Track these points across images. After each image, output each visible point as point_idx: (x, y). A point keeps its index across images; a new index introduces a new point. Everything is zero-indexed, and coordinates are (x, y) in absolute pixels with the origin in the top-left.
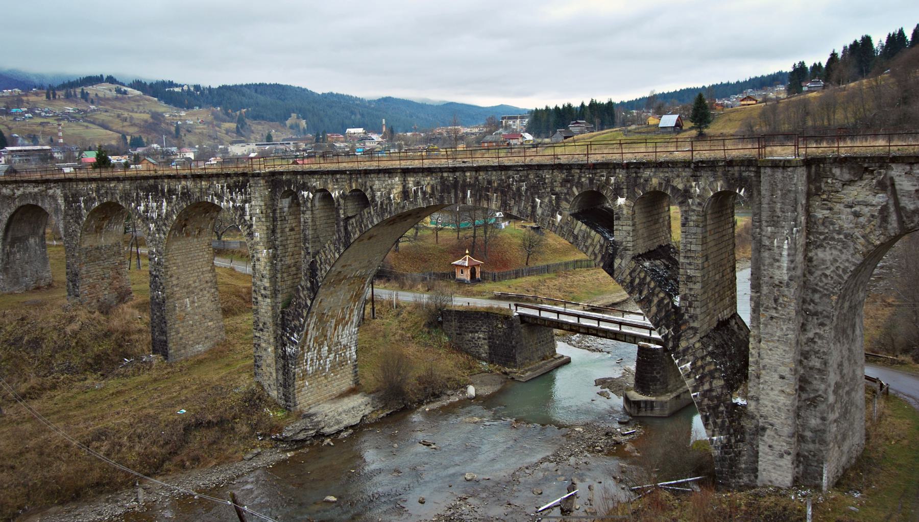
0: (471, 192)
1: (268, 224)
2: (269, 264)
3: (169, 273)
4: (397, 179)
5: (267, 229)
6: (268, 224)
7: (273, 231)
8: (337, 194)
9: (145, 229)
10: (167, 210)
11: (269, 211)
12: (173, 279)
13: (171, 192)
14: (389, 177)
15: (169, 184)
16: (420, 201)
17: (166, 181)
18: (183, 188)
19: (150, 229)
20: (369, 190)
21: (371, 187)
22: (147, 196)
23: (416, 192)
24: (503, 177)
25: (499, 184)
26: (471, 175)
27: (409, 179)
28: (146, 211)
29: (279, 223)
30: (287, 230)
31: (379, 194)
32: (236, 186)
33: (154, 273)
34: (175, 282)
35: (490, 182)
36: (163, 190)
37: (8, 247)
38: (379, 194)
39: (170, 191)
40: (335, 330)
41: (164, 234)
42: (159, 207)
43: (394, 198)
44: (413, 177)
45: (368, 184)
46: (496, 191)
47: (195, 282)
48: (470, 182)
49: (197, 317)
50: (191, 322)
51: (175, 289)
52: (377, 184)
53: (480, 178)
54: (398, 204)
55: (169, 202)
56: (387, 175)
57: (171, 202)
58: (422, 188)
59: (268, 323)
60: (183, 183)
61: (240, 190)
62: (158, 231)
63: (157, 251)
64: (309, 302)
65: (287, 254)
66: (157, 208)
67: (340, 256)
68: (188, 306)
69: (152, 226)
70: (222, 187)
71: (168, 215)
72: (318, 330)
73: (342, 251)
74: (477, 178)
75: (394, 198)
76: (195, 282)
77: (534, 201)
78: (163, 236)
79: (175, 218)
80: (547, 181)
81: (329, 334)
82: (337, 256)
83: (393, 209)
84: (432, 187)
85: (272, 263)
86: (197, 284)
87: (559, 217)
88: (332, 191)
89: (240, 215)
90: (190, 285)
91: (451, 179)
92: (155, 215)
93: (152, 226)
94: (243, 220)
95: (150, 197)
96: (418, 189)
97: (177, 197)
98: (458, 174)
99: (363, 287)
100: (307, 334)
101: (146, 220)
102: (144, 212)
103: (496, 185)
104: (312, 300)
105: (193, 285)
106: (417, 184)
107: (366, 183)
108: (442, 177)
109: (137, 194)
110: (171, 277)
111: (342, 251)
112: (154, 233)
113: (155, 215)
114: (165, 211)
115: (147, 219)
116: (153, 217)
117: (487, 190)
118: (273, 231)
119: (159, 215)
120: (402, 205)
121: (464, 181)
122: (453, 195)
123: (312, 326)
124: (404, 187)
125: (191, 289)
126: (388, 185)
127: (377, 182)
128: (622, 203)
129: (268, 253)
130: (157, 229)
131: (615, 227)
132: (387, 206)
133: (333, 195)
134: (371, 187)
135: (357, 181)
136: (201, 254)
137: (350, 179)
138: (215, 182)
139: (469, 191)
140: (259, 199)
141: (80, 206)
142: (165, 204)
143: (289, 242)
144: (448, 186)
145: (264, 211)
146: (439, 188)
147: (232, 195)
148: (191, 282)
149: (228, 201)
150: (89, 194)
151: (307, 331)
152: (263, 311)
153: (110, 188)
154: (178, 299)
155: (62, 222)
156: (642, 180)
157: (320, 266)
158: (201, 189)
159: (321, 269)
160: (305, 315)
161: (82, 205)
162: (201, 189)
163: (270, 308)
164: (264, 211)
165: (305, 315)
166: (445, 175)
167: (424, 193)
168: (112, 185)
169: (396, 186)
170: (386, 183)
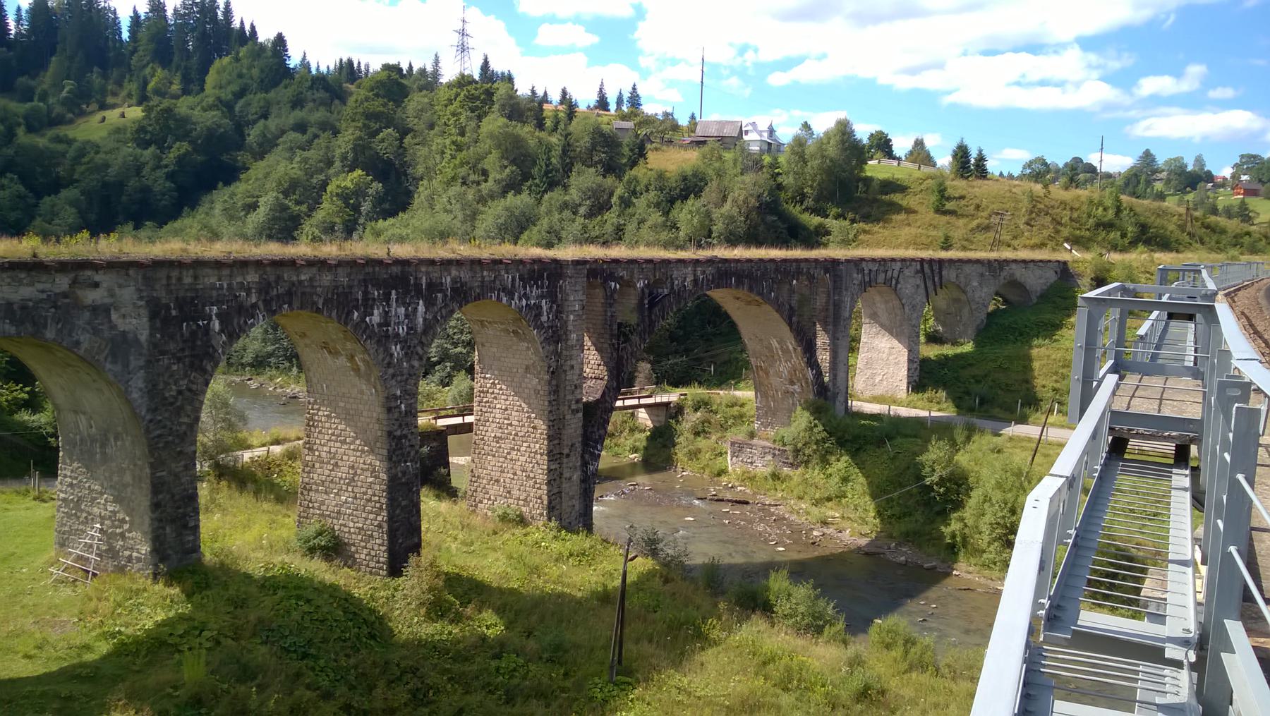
9: (381, 357)
10: (425, 320)
13: (434, 287)
15: (427, 273)
17: (423, 269)
18: (454, 281)
19: (392, 355)
22: (387, 298)
28: (385, 323)
32: (531, 278)
33: (398, 433)
35: (744, 271)
36: (418, 285)
38: (676, 282)
39: (430, 285)
46: (746, 277)
52: (675, 274)
55: (429, 304)
57: (434, 304)
59: (577, 445)
61: (536, 283)
66: (407, 316)
69: (396, 350)
78: (416, 363)
89: (536, 316)
92: (402, 330)
93: (396, 350)
95: (394, 296)
97: (445, 296)
102: (380, 325)
106: (704, 272)
109: (366, 293)
113: (402, 330)
114: (421, 320)
115: (387, 336)
116: (398, 335)
119: (410, 328)
124: (695, 275)
130: (406, 354)
137: (655, 269)
138: (503, 272)
140: (581, 292)
141: (207, 329)
142: (421, 308)
147: (525, 288)
149: (520, 299)
153: (300, 282)
158: (483, 282)
161: (216, 325)
162: (483, 282)
167: (708, 280)
168: (303, 278)
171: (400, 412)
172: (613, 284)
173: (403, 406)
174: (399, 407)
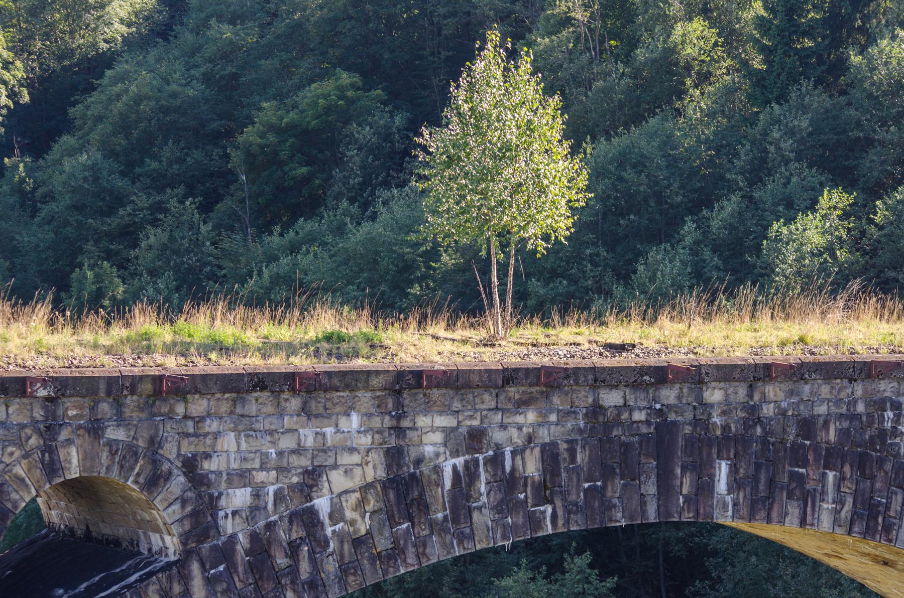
0: (734, 470)
4: (355, 421)
14: (305, 411)
16: (482, 519)
20: (178, 483)
21: (190, 466)
24: (861, 408)
25: (843, 434)
26: (727, 401)
27: (423, 421)
31: (240, 497)
35: (807, 426)
43: (336, 515)
44: (446, 410)
45: (170, 450)
48: (726, 428)
53: (768, 410)
54: (358, 542)
56: (295, 403)
58: (496, 461)
74: (753, 410)
75: (336, 515)
83: (331, 566)
84: (550, 455)
91: (638, 416)
96: (471, 470)
98: (669, 395)
103: (832, 435)
107: (155, 443)
108: (596, 410)
117: (798, 456)
120: (382, 544)
121: (701, 423)
122: (650, 488)
124: (394, 456)
126: (299, 451)
127: (228, 442)
132: (293, 549)
134: (190, 466)
135: (95, 429)
144: (626, 447)
146: (581, 457)
166: (611, 398)
169: (346, 459)
170: (287, 443)
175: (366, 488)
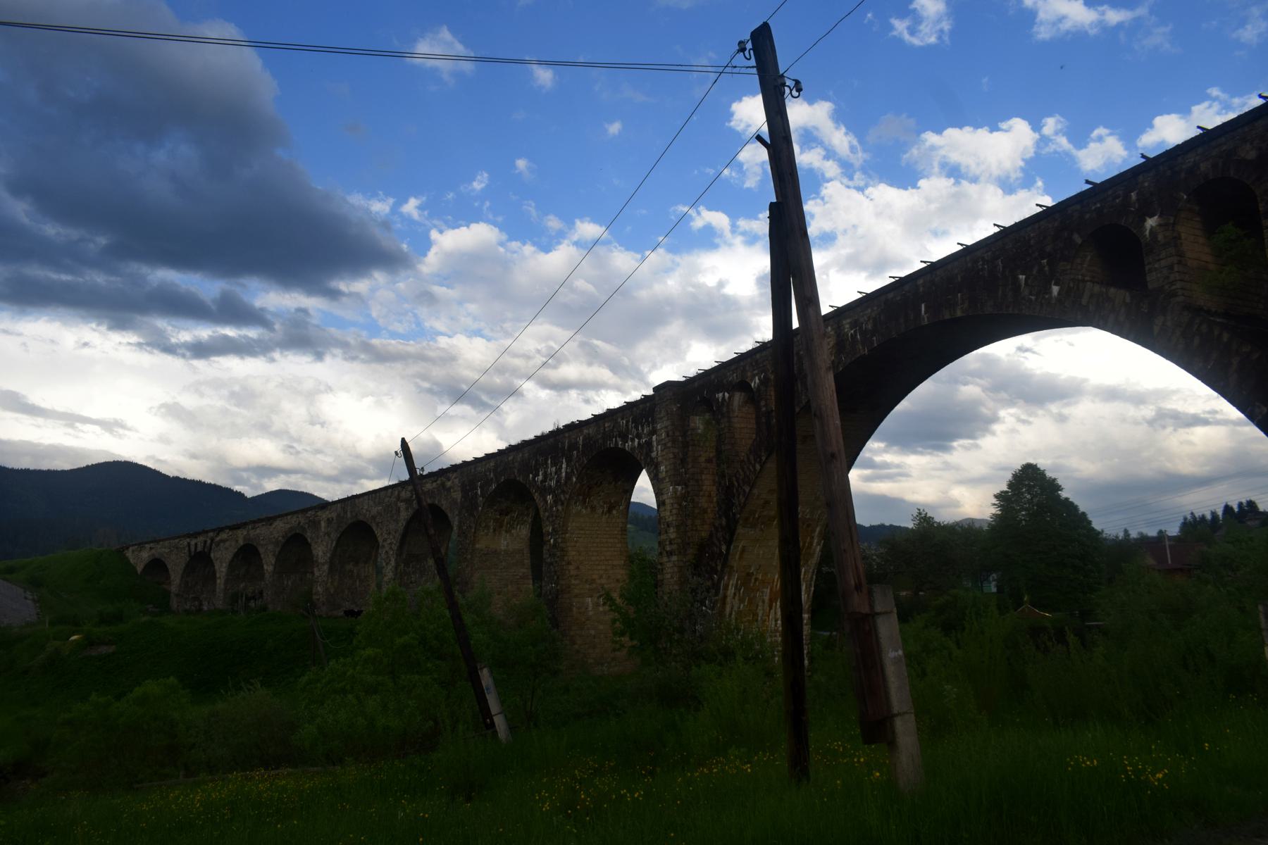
1: (676, 451)
2: (676, 506)
3: (566, 558)
5: (675, 457)
6: (676, 451)
7: (683, 461)
8: (757, 381)
10: (566, 472)
11: (677, 433)
12: (571, 567)
13: (573, 446)
23: (854, 336)
29: (690, 449)
30: (702, 459)
34: (573, 573)
37: (403, 565)
40: (771, 608)
41: (562, 504)
42: (558, 472)
47: (601, 577)
49: (601, 627)
50: (593, 632)
51: (573, 582)
60: (586, 431)
61: (647, 420)
62: (556, 502)
63: (553, 529)
64: (724, 548)
65: (701, 493)
66: (556, 473)
67: (762, 467)
68: (590, 609)
69: (549, 498)
70: (627, 422)
71: (568, 477)
72: (741, 601)
73: (764, 458)
76: (601, 577)
77: (1016, 279)
78: (560, 508)
79: (574, 479)
80: (1032, 242)
81: (760, 613)
82: (758, 467)
85: (680, 505)
86: (603, 581)
87: (1055, 289)
88: (752, 380)
90: (594, 580)
92: (553, 483)
93: (549, 498)
94: (649, 460)
99: (811, 543)
100: (724, 603)
101: (544, 491)
103: (959, 279)
104: (729, 544)
105: (599, 581)
110: (569, 563)
111: (764, 458)
112: (552, 507)
114: (564, 474)
118: (683, 461)
123: (731, 591)
125: (594, 586)
128: (1154, 225)
129: (675, 491)
130: (554, 501)
131: (1147, 268)
133: (753, 385)
136: (612, 540)
139: (923, 306)
142: (564, 466)
143: (704, 477)
145: (670, 433)
148: (594, 577)
149: (633, 440)
150: (486, 475)
151: (725, 597)
152: (669, 576)
154: (576, 596)
155: (457, 518)
156: (1183, 175)
157: (737, 490)
159: (739, 495)
160: (719, 568)
163: (676, 569)
164: (670, 433)
165: (719, 568)
171: (550, 544)
172: (721, 395)
173: (552, 541)
174: (549, 541)
175: (833, 346)
